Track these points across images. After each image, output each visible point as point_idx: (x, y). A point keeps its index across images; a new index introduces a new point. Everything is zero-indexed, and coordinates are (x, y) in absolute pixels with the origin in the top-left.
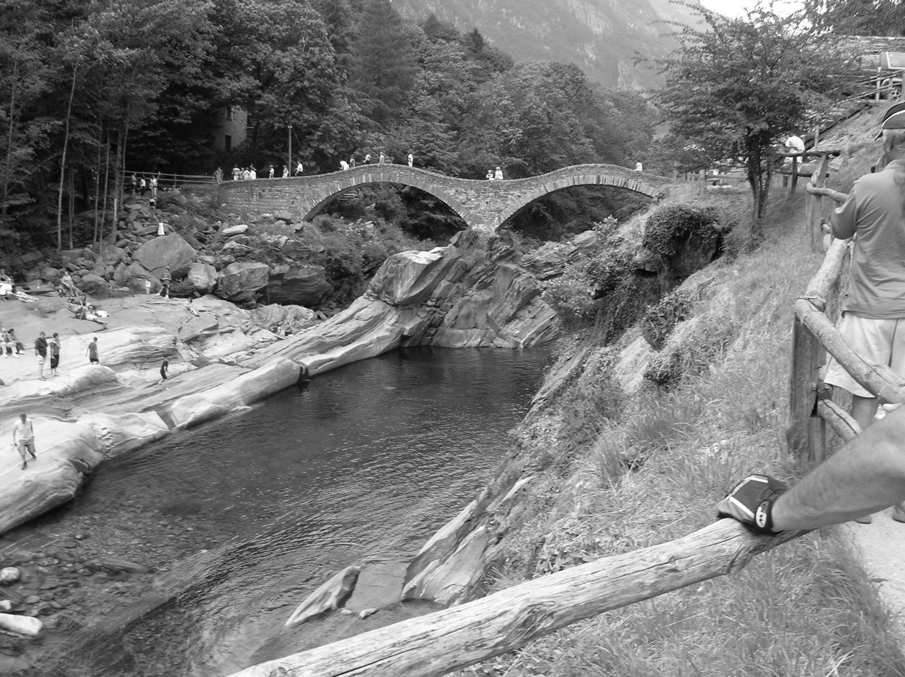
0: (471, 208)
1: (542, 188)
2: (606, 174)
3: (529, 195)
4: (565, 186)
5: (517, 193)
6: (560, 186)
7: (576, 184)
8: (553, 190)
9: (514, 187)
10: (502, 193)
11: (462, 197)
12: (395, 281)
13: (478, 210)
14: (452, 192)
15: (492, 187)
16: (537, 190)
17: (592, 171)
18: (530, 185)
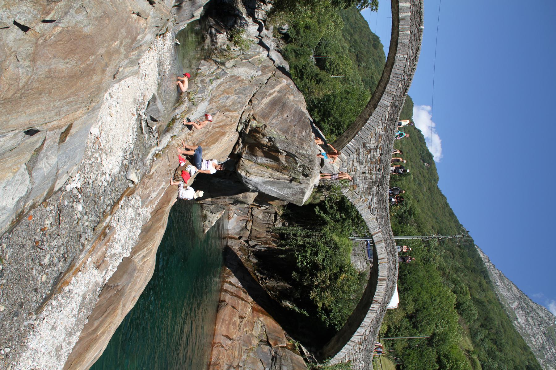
0: (358, 154)
1: (377, 230)
2: (387, 284)
3: (371, 217)
4: (378, 251)
5: (374, 205)
6: (378, 246)
7: (379, 261)
8: (375, 240)
9: (381, 201)
10: (375, 189)
11: (372, 144)
12: (272, 163)
13: (356, 164)
14: (380, 131)
15: (383, 177)
16: (376, 224)
17: (392, 274)
18: (382, 218)
